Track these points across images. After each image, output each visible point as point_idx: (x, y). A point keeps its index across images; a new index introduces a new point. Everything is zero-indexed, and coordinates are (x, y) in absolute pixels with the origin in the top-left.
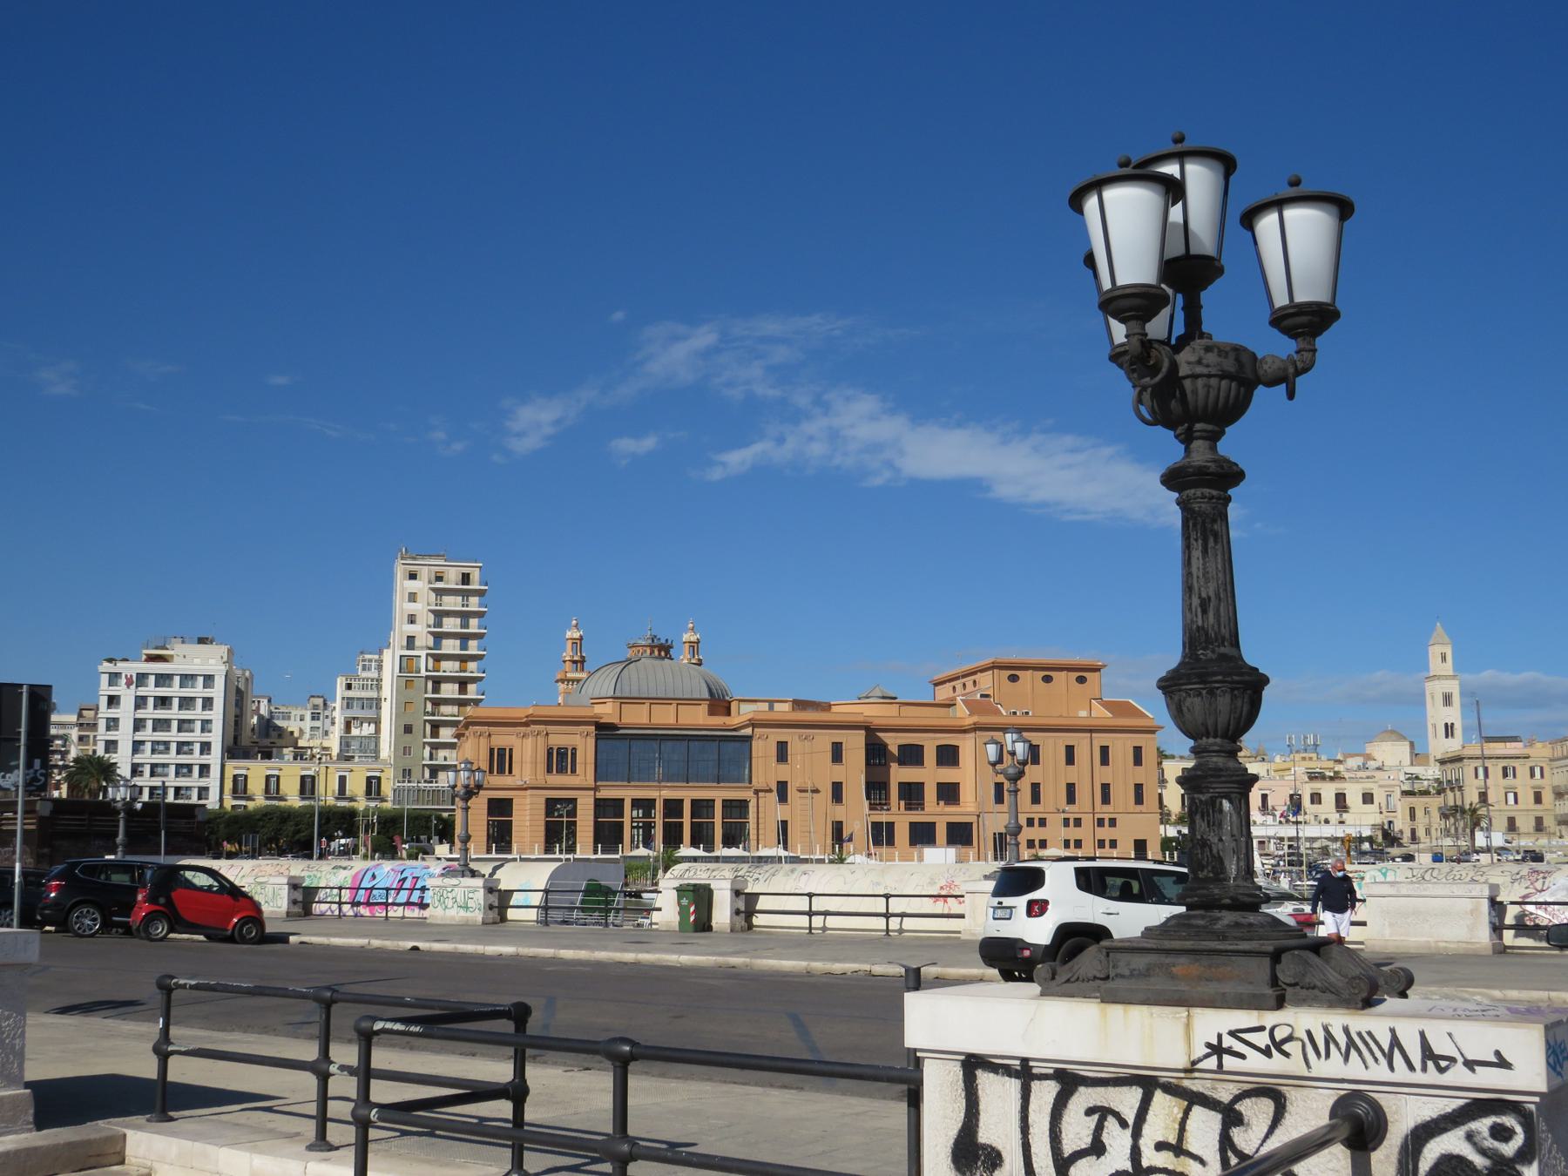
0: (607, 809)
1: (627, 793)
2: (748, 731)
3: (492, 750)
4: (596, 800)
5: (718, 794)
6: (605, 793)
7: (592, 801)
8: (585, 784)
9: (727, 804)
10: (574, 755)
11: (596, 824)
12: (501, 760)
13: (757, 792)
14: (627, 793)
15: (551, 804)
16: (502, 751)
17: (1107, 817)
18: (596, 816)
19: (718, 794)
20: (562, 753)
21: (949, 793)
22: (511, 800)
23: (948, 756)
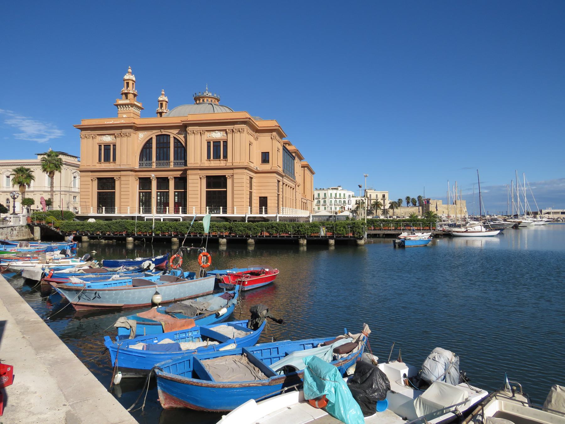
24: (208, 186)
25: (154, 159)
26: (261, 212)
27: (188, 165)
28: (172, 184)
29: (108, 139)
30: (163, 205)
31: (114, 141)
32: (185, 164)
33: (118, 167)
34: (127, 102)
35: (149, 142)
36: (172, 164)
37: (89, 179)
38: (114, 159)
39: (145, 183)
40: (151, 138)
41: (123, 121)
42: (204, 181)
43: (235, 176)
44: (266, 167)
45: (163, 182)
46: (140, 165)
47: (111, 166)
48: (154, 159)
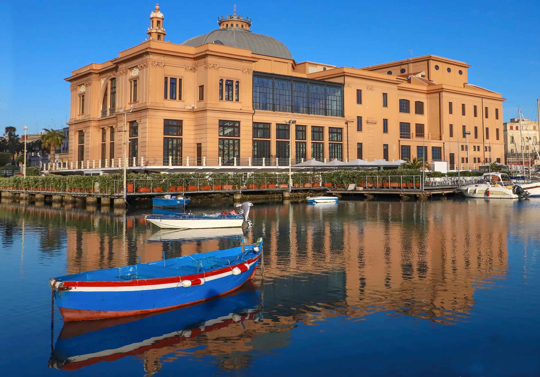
0: (262, 129)
1: (274, 119)
3: (166, 78)
4: (254, 123)
5: (327, 122)
7: (251, 124)
8: (245, 109)
9: (332, 130)
10: (237, 86)
11: (254, 141)
12: (173, 88)
13: (347, 123)
14: (274, 119)
15: (223, 124)
16: (173, 80)
17: (488, 145)
18: (253, 137)
19: (327, 122)
20: (229, 84)
21: (420, 129)
22: (181, 121)
23: (420, 108)
26: (166, 162)
30: (318, 154)
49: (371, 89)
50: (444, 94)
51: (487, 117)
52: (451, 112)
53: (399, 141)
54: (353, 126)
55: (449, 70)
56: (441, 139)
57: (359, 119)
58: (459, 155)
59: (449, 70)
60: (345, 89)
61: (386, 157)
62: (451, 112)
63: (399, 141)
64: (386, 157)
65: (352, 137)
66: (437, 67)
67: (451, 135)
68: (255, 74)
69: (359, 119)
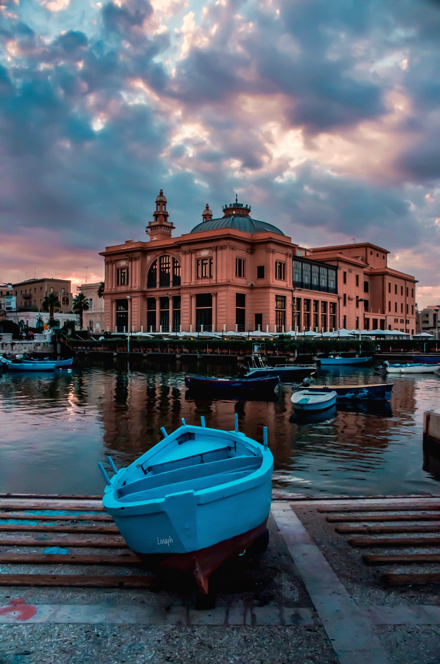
2: (334, 264)
3: (236, 259)
4: (293, 298)
6: (297, 294)
13: (339, 300)
14: (303, 295)
16: (240, 260)
24: (197, 306)
25: (158, 280)
27: (182, 284)
28: (171, 302)
29: (123, 263)
31: (127, 265)
32: (179, 284)
33: (129, 289)
34: (157, 223)
35: (154, 264)
36: (171, 284)
37: (109, 301)
38: (128, 283)
39: (151, 303)
40: (156, 261)
41: (134, 246)
42: (194, 300)
43: (219, 294)
44: (261, 282)
45: (164, 301)
46: (149, 286)
47: (123, 288)
48: (158, 280)
49: (350, 271)
50: (387, 277)
51: (407, 296)
52: (390, 291)
53: (364, 314)
54: (342, 301)
55: (378, 255)
56: (383, 312)
57: (345, 295)
58: (394, 325)
59: (378, 255)
60: (338, 271)
61: (357, 327)
62: (390, 291)
63: (364, 314)
64: (357, 327)
65: (343, 311)
66: (371, 253)
67: (390, 310)
68: (294, 258)
69: (345, 295)
